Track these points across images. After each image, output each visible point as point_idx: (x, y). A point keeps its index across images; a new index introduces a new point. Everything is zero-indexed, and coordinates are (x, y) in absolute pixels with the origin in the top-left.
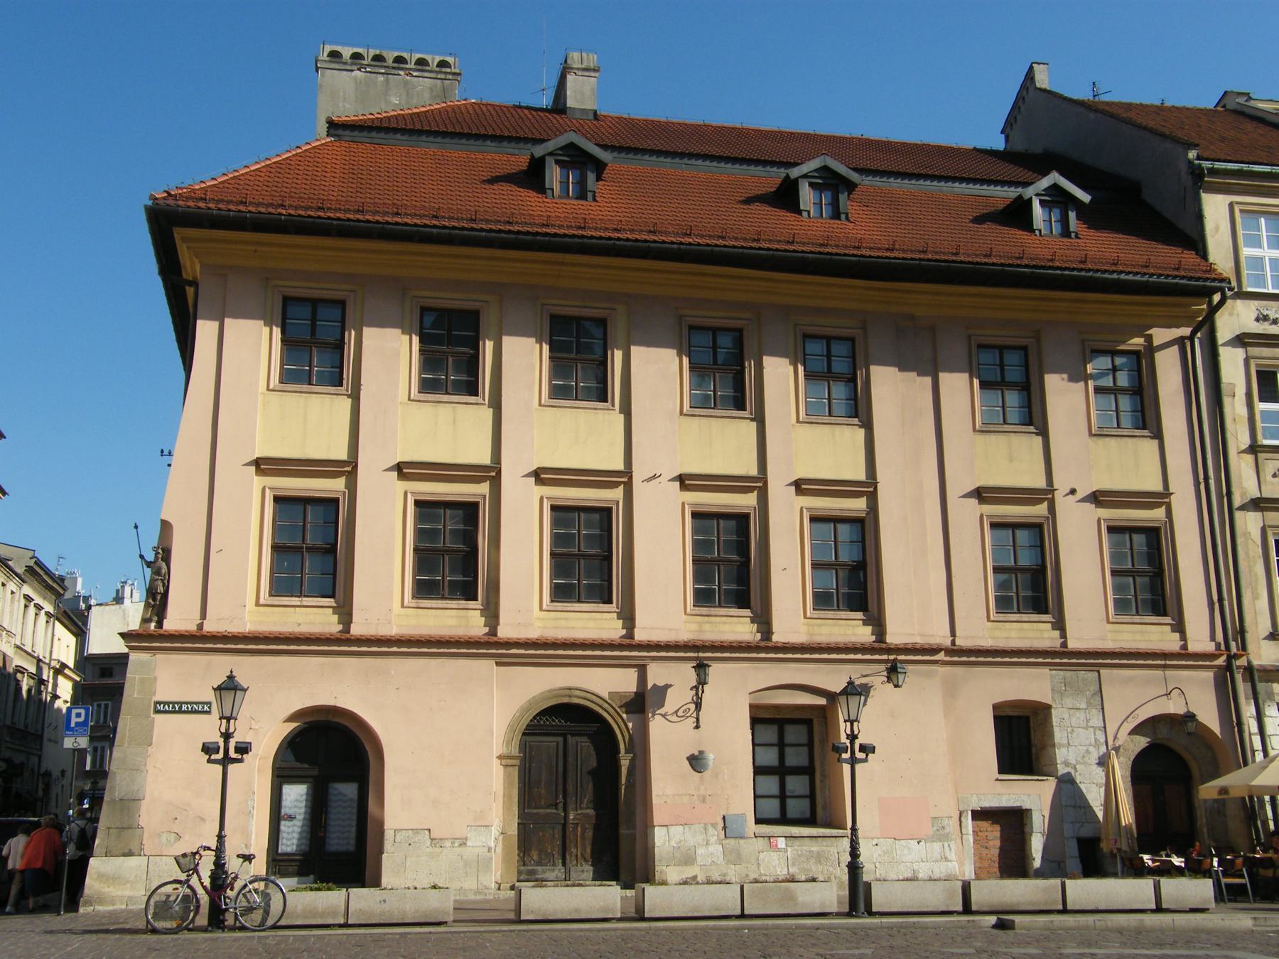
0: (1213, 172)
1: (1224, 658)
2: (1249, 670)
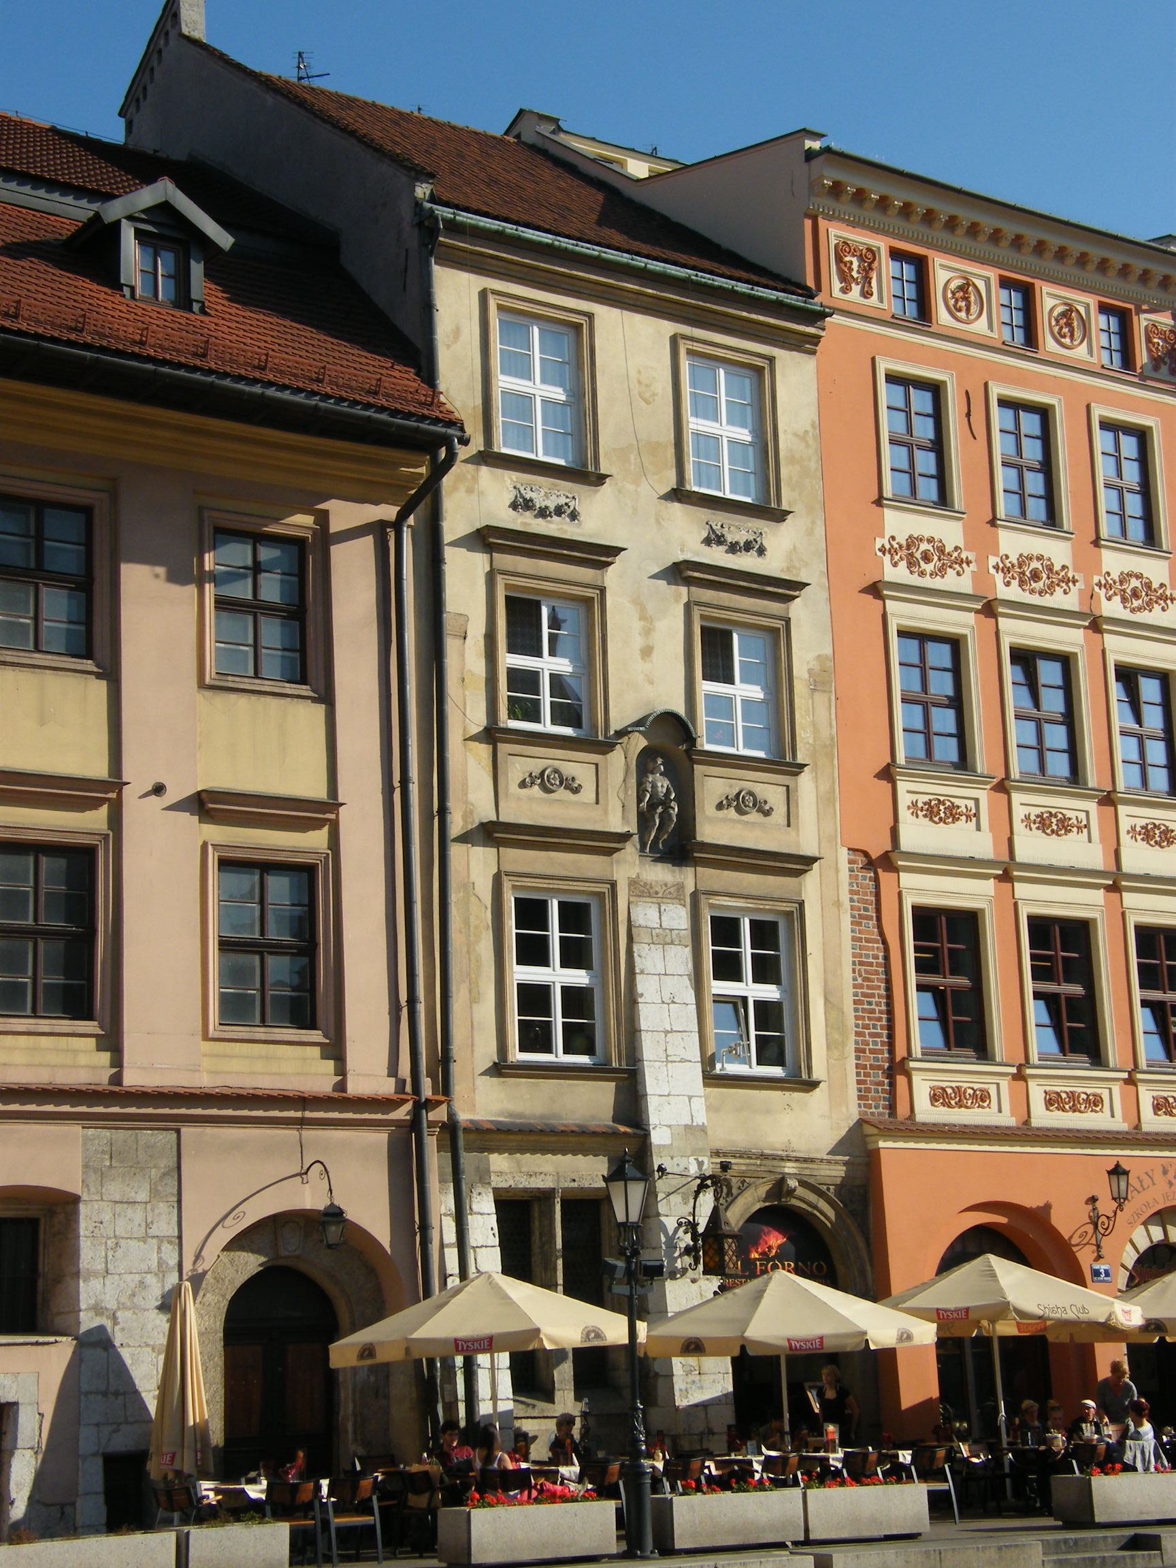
0: (454, 228)
1: (408, 1106)
2: (450, 1128)
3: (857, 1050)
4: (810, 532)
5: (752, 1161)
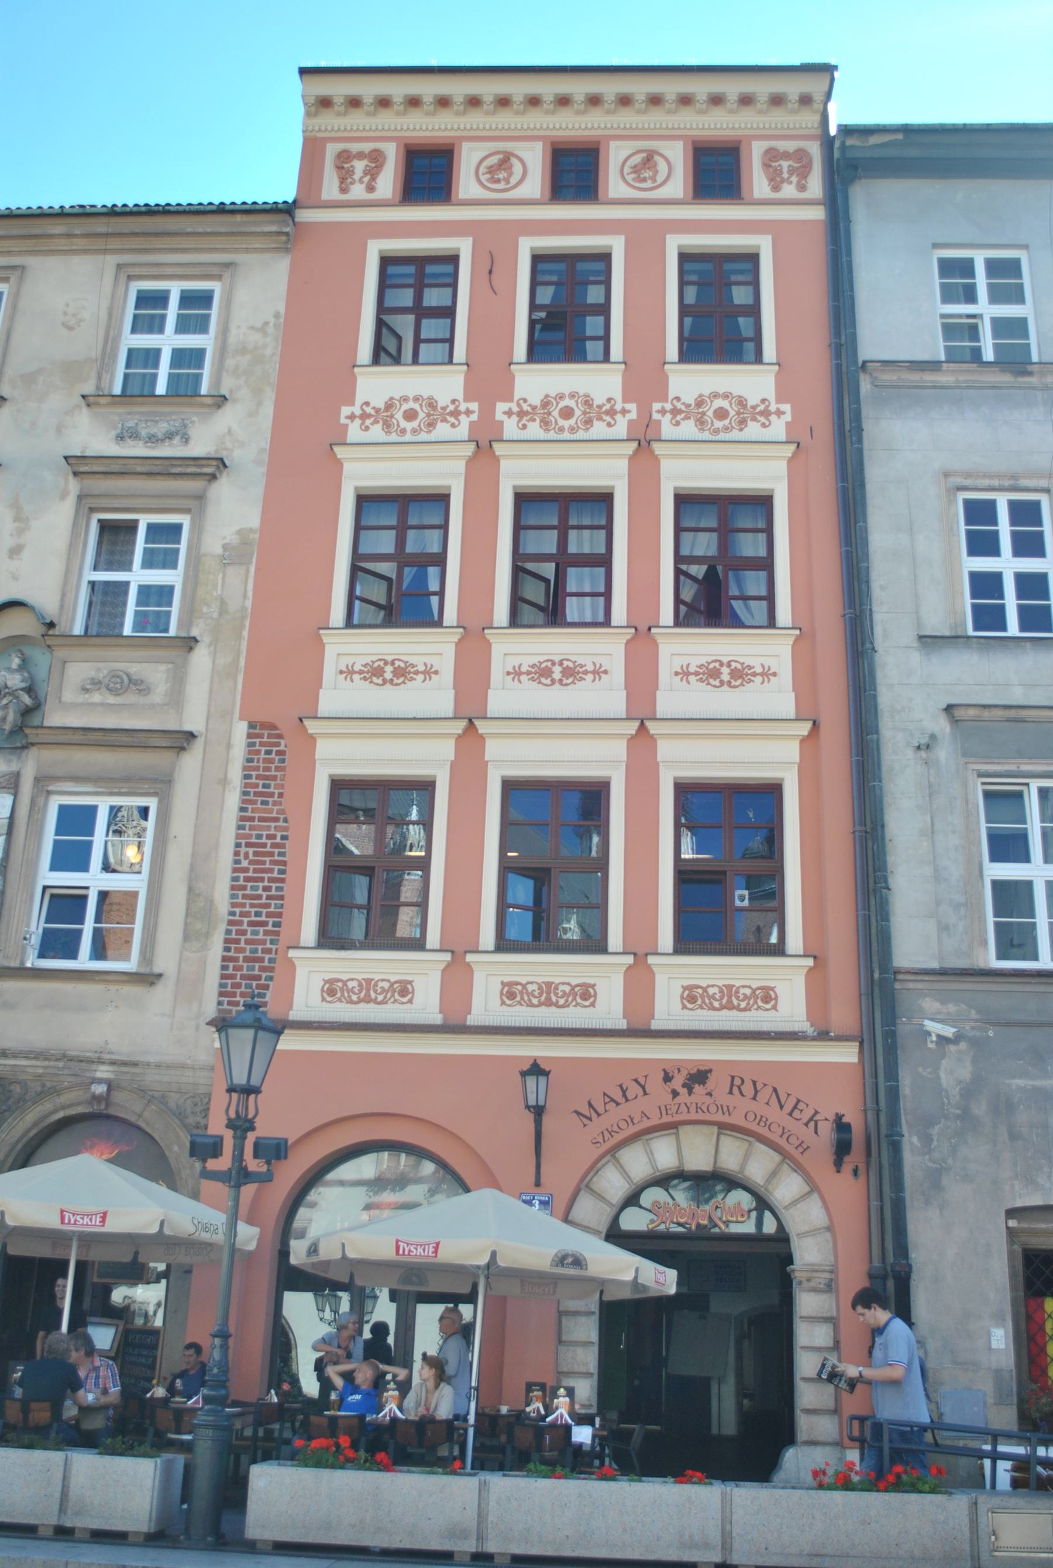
3: (226, 941)
4: (253, 414)
5: (52, 1063)
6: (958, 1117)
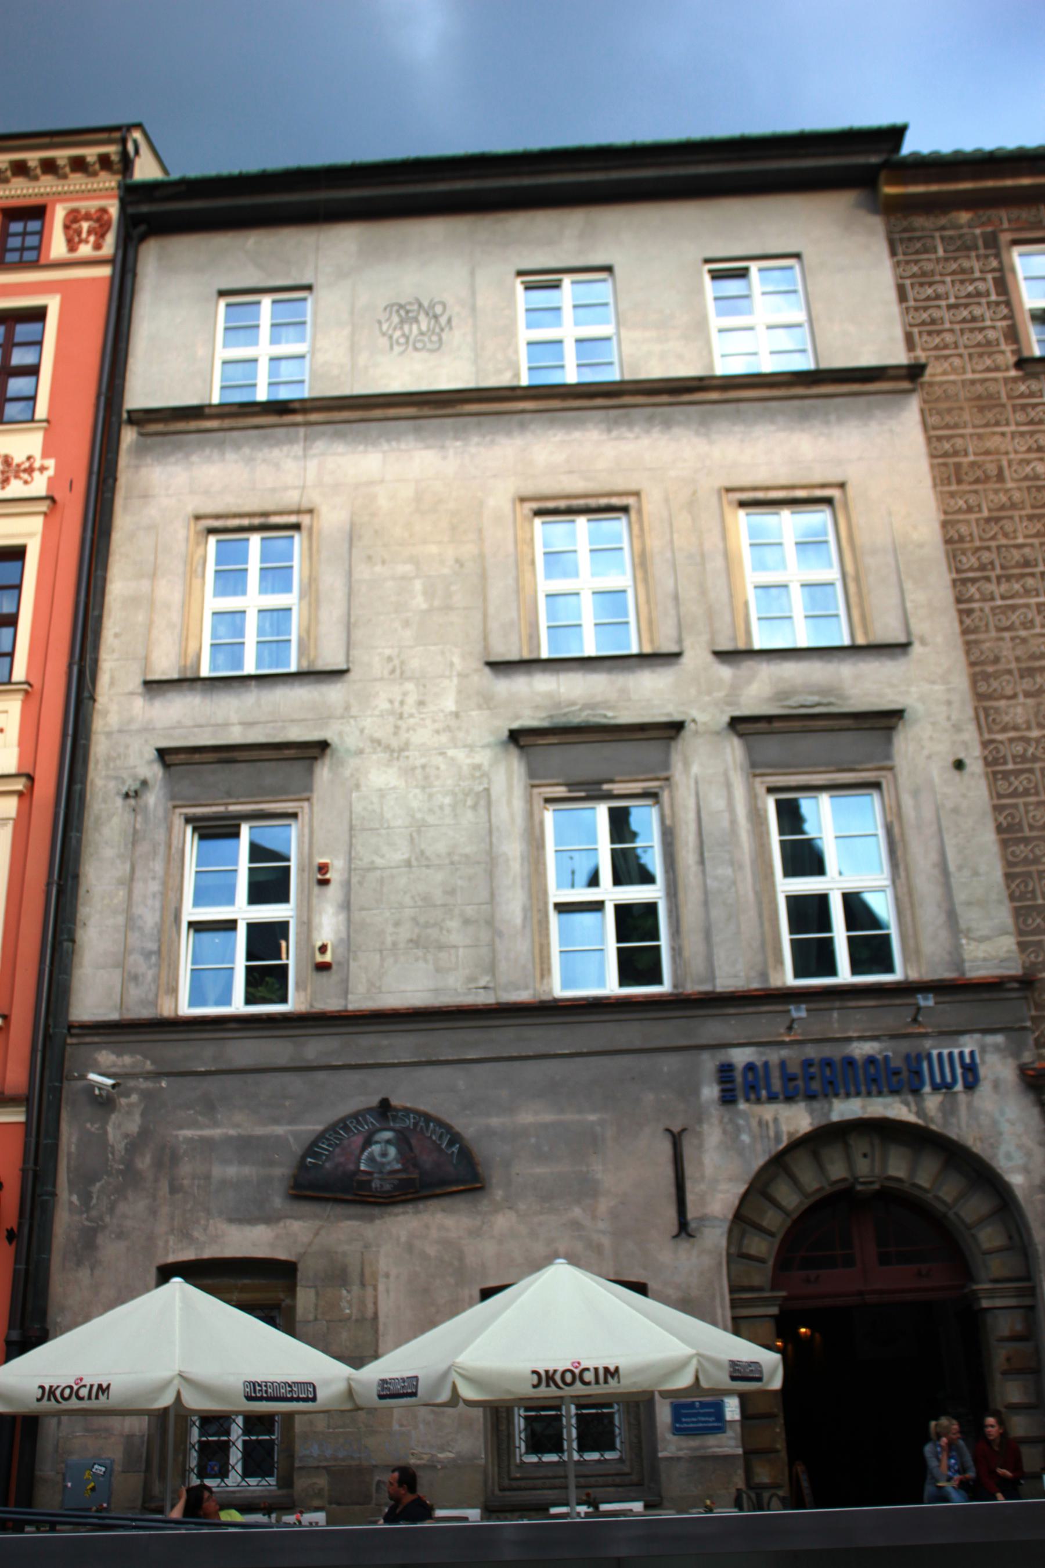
6: (120, 1172)
